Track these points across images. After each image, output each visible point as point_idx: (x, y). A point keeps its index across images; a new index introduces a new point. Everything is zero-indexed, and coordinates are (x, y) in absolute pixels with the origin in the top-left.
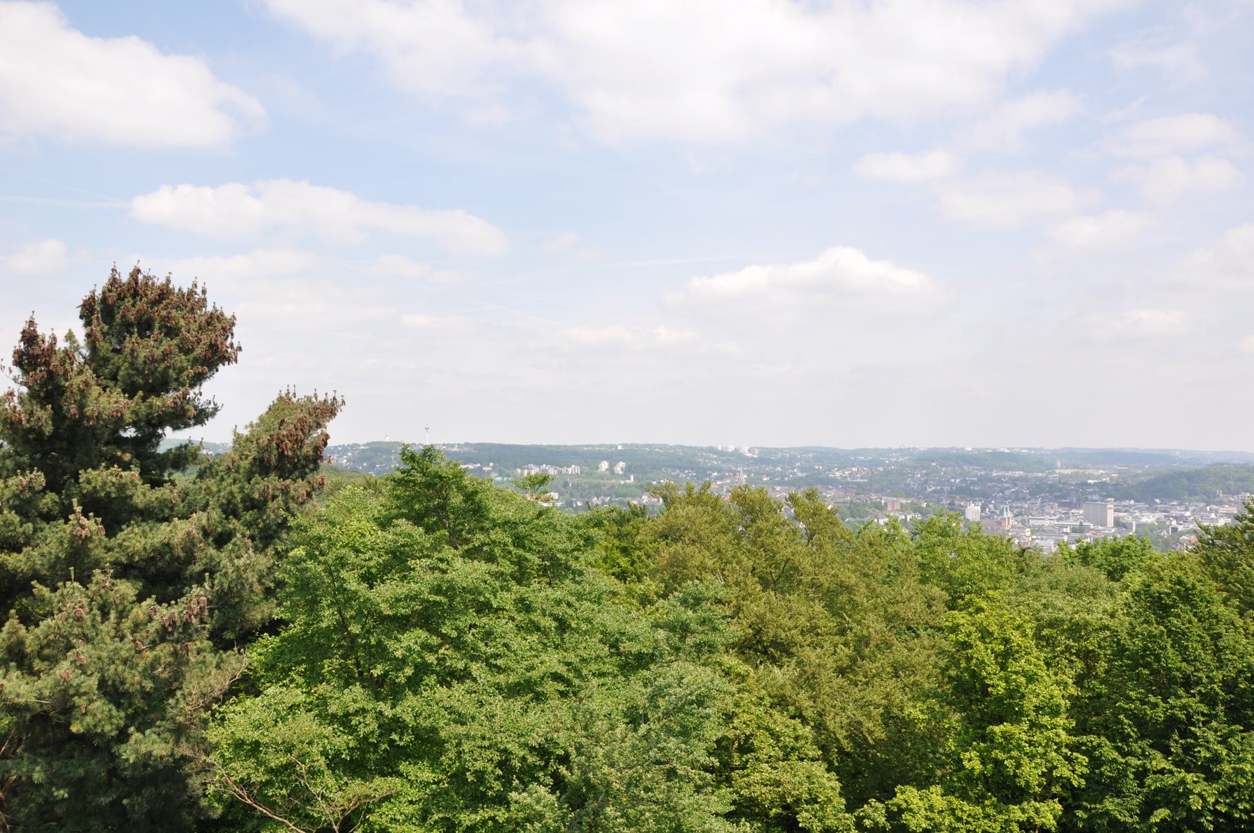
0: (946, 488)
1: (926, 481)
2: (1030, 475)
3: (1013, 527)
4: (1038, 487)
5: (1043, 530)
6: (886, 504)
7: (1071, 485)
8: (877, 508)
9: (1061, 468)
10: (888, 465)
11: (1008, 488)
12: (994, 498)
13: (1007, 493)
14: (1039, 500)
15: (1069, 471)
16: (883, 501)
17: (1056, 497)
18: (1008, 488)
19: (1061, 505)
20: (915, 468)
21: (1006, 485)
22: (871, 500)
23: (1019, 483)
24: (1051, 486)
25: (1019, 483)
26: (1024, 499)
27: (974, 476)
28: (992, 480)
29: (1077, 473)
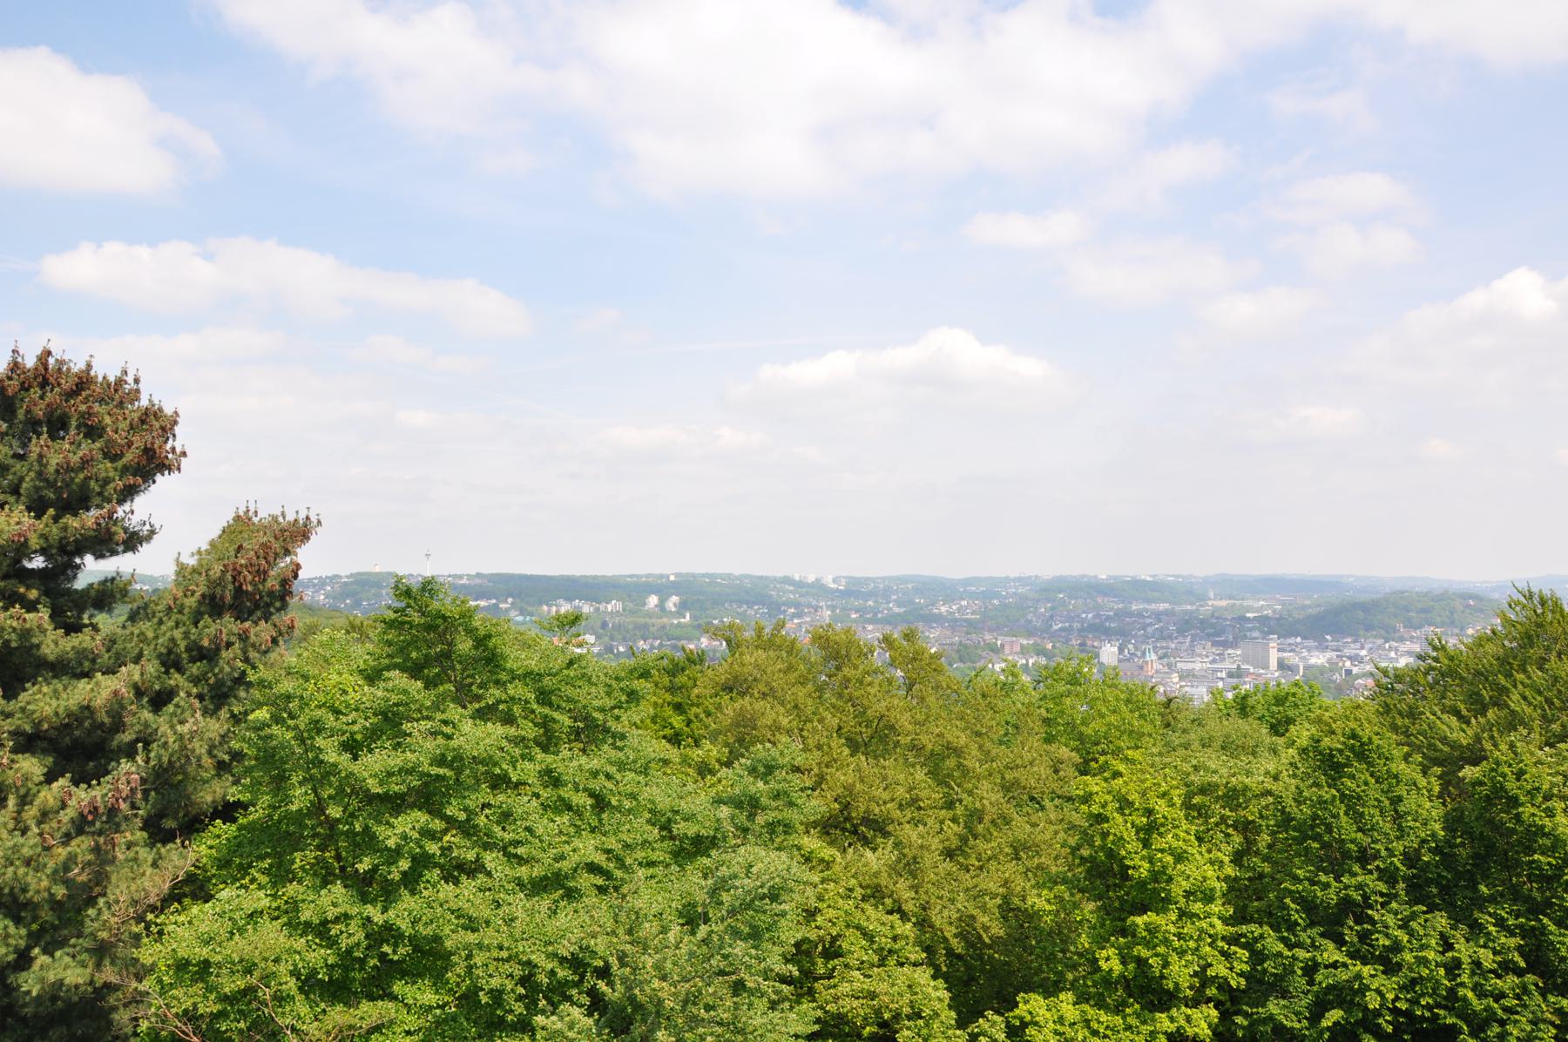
0: (1076, 625)
2: (1178, 608)
3: (1157, 672)
4: (1187, 622)
5: (1194, 676)
6: (1003, 646)
7: (1226, 619)
8: (992, 650)
9: (1214, 600)
10: (1005, 597)
12: (1134, 637)
13: (1150, 630)
15: (1223, 603)
16: (999, 643)
17: (1209, 635)
19: (1215, 644)
20: (1038, 601)
21: (1148, 621)
22: (984, 641)
23: (1163, 617)
24: (1202, 622)
25: (1163, 617)
26: (1170, 637)
27: (1111, 610)
28: (1131, 614)
29: (1234, 605)
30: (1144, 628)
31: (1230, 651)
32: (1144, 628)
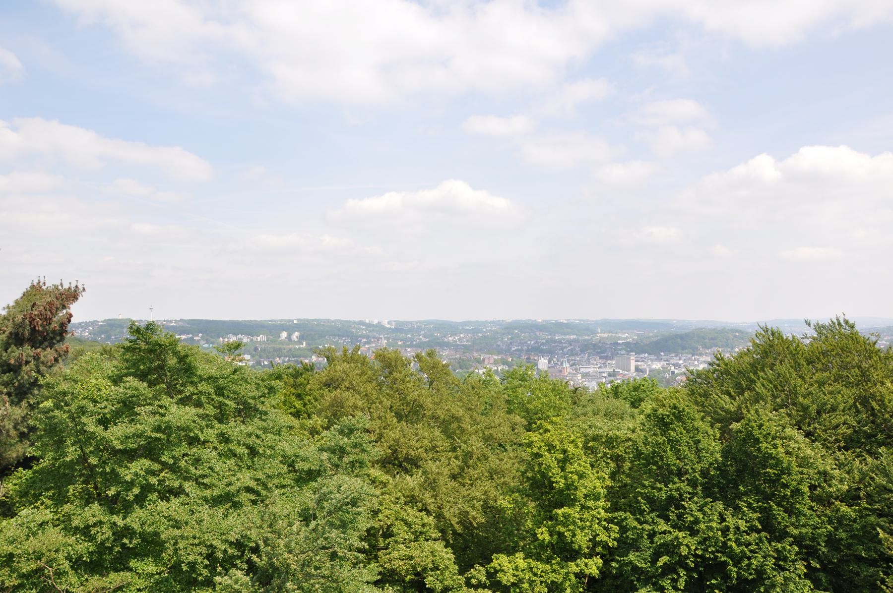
0: (525, 348)
1: (511, 343)
2: (580, 338)
4: (586, 346)
5: (590, 375)
6: (484, 359)
7: (607, 344)
9: (601, 333)
11: (566, 347)
12: (557, 354)
13: (565, 350)
14: (587, 355)
15: (606, 335)
16: (482, 358)
18: (566, 347)
19: (601, 358)
21: (564, 345)
22: (473, 356)
24: (594, 345)
26: (577, 354)
28: (555, 342)
29: (611, 336)
30: (562, 350)
31: (609, 362)
32: (562, 350)
